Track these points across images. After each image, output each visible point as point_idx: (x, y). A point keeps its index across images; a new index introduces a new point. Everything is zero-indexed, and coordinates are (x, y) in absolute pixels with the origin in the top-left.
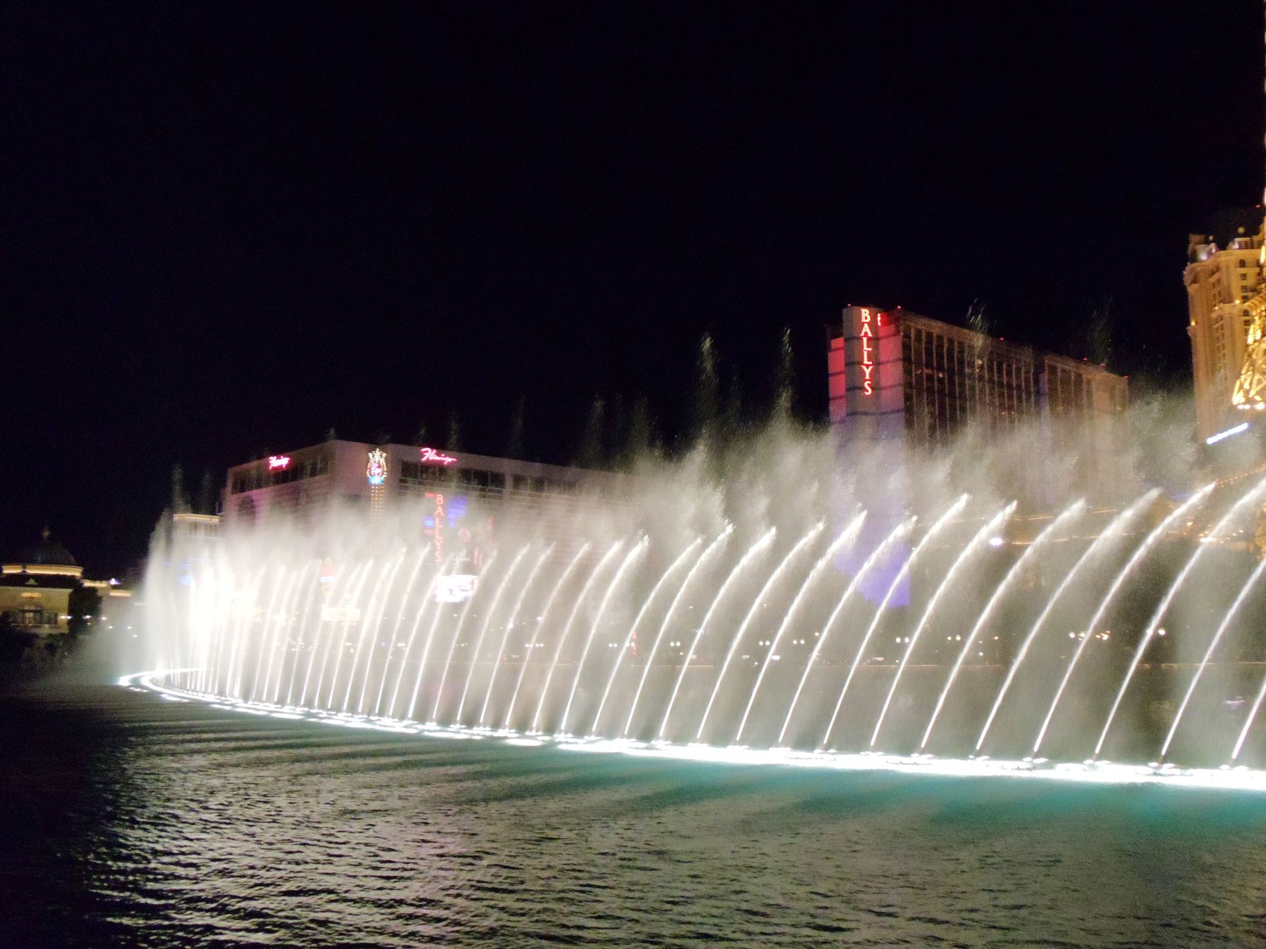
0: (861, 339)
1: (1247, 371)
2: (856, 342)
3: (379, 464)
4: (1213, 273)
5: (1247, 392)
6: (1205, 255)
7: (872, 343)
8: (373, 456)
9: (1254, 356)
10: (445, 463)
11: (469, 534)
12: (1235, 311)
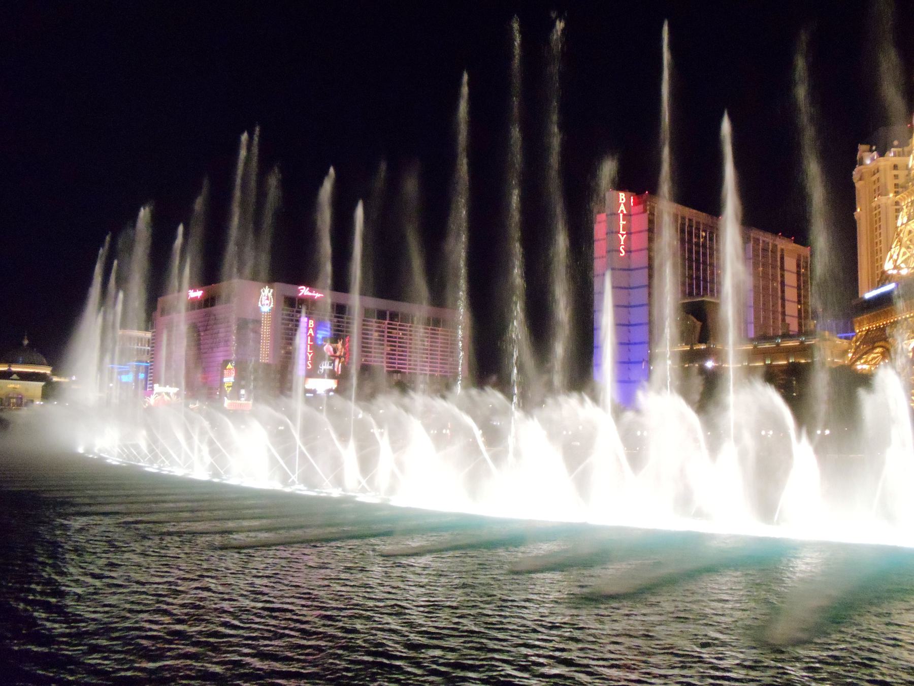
1: (896, 246)
3: (268, 297)
4: (874, 174)
5: (896, 261)
6: (868, 159)
8: (264, 291)
9: (901, 235)
11: (331, 349)
12: (889, 202)
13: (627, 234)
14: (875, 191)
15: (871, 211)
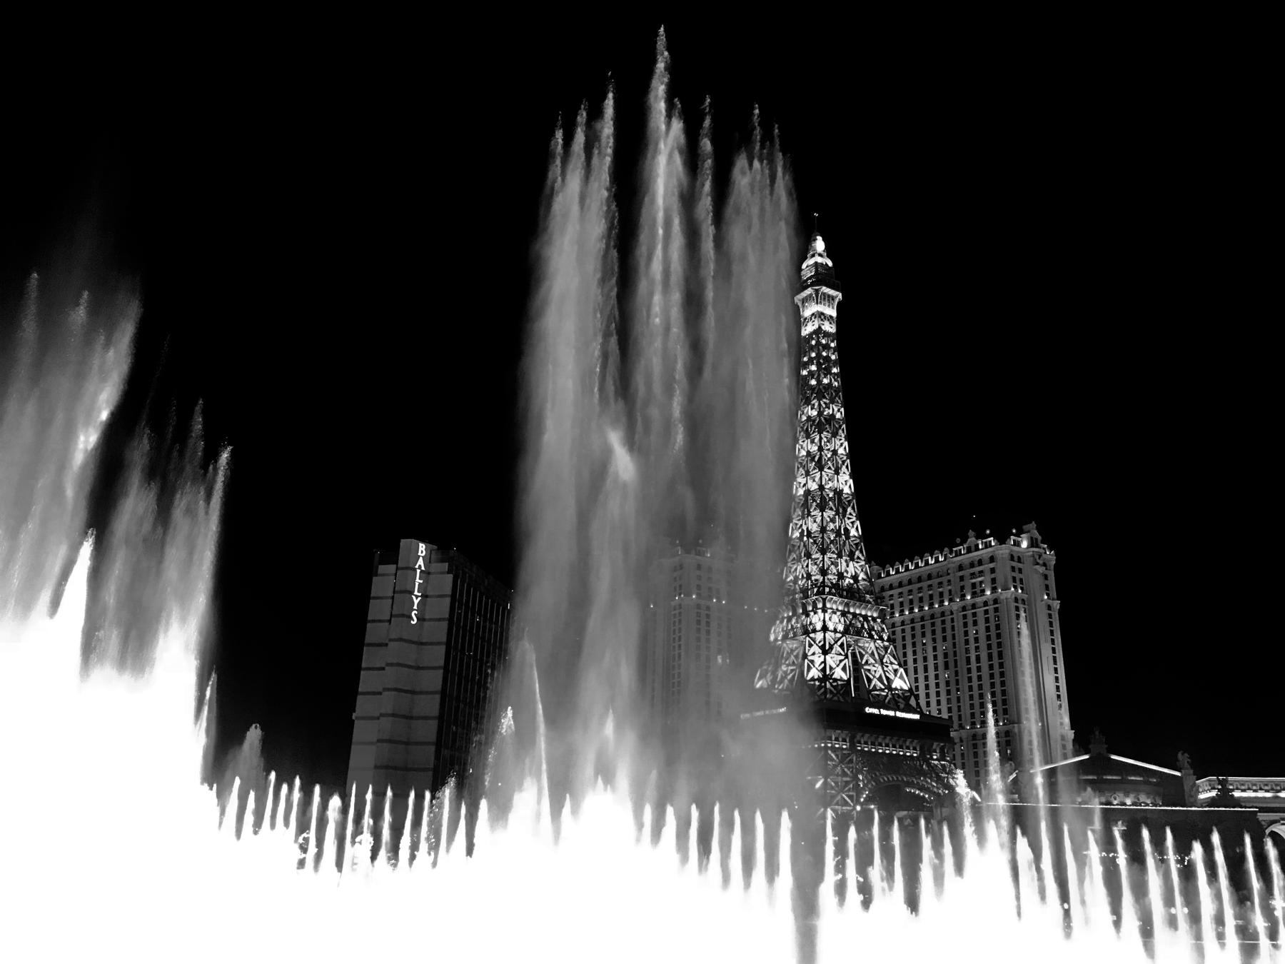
0: (415, 570)
2: (410, 572)
7: (424, 575)
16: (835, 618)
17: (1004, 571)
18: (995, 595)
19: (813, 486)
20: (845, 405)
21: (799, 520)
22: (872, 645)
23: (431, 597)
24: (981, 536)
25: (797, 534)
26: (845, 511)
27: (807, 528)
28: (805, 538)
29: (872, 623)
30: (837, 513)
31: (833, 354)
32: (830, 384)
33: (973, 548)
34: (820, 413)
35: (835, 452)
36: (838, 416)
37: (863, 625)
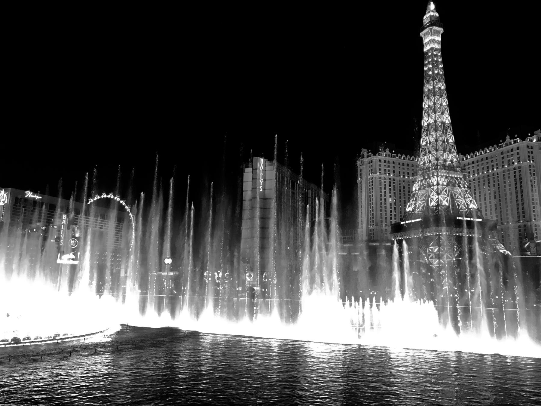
3: (3, 196)
4: (369, 163)
10: (36, 199)
13: (264, 180)
14: (369, 171)
15: (367, 181)
16: (443, 179)
17: (524, 153)
18: (519, 165)
19: (431, 121)
20: (446, 82)
21: (425, 137)
22: (460, 190)
23: (267, 180)
24: (512, 138)
25: (424, 143)
26: (446, 130)
27: (429, 140)
28: (428, 145)
29: (460, 180)
30: (443, 132)
31: (440, 58)
32: (438, 73)
33: (508, 144)
34: (434, 87)
35: (441, 105)
36: (442, 88)
37: (455, 181)
